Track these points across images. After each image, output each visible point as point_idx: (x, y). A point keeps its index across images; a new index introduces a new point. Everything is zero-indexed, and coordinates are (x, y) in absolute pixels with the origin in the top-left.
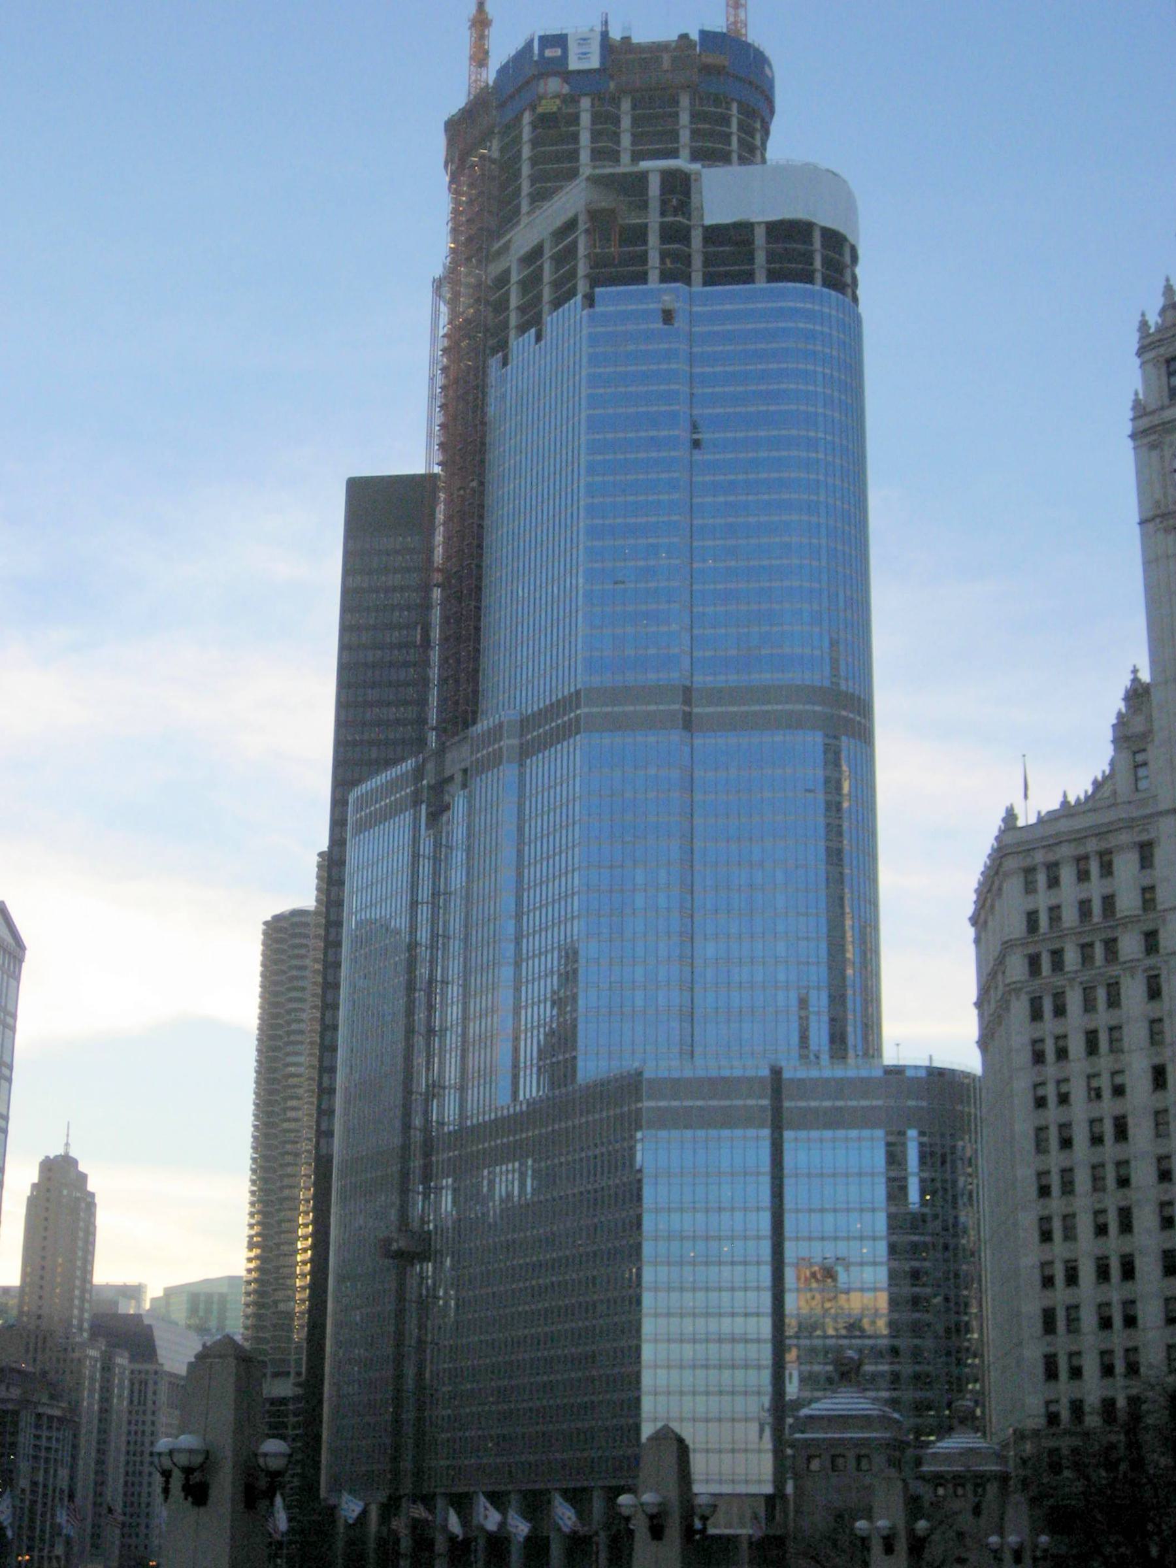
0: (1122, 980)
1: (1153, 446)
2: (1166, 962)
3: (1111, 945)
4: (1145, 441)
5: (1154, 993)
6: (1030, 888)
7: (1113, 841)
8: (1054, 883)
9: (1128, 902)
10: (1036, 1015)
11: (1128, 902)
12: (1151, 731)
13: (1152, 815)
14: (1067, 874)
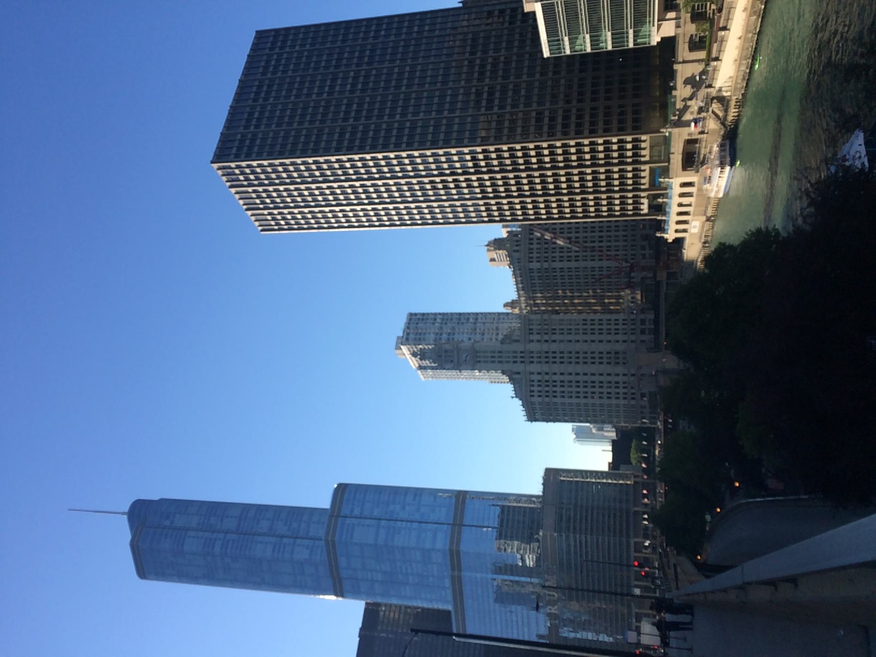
1: (461, 365)
5: (555, 374)
6: (533, 396)
8: (533, 391)
9: (539, 377)
11: (539, 377)
14: (532, 388)
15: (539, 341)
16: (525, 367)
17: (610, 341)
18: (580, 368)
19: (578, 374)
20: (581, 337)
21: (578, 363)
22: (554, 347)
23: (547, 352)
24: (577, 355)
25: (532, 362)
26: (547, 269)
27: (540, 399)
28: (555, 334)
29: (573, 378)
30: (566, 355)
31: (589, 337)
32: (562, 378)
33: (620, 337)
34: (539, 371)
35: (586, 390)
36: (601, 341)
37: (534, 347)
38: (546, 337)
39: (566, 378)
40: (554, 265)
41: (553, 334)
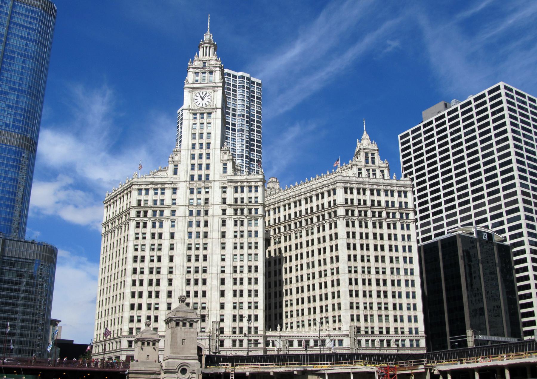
0: (164, 222)
2: (177, 219)
3: (162, 212)
4: (188, 90)
5: (173, 226)
7: (166, 186)
9: (168, 202)
10: (138, 227)
12: (180, 161)
13: (178, 181)
15: (224, 201)
16: (184, 182)
17: (222, 307)
18: (180, 262)
19: (171, 259)
20: (229, 264)
21: (189, 260)
22: (215, 223)
23: (206, 213)
24: (200, 270)
25: (192, 192)
26: (335, 215)
27: (134, 203)
28: (236, 225)
29: (165, 253)
30: (201, 241)
31: (229, 277)
32: (166, 236)
33: (228, 325)
34: (177, 202)
35: (146, 271)
36: (222, 294)
37: (215, 195)
38: (230, 211)
39: (166, 242)
40: (341, 223)
41: (236, 222)
